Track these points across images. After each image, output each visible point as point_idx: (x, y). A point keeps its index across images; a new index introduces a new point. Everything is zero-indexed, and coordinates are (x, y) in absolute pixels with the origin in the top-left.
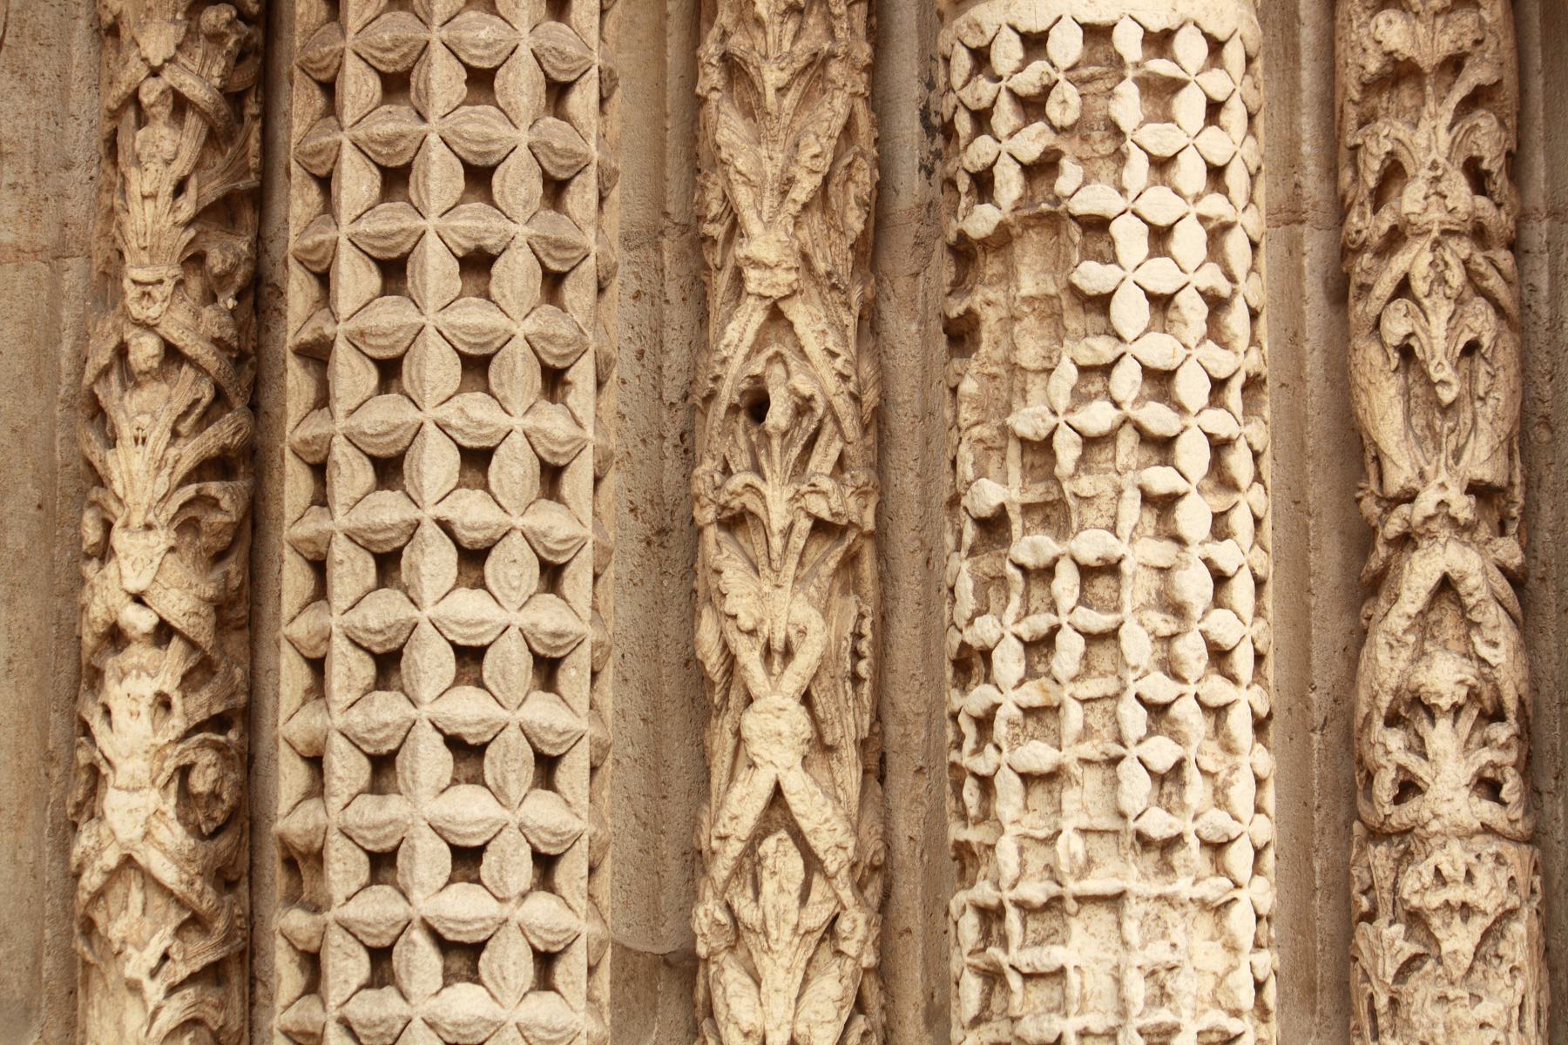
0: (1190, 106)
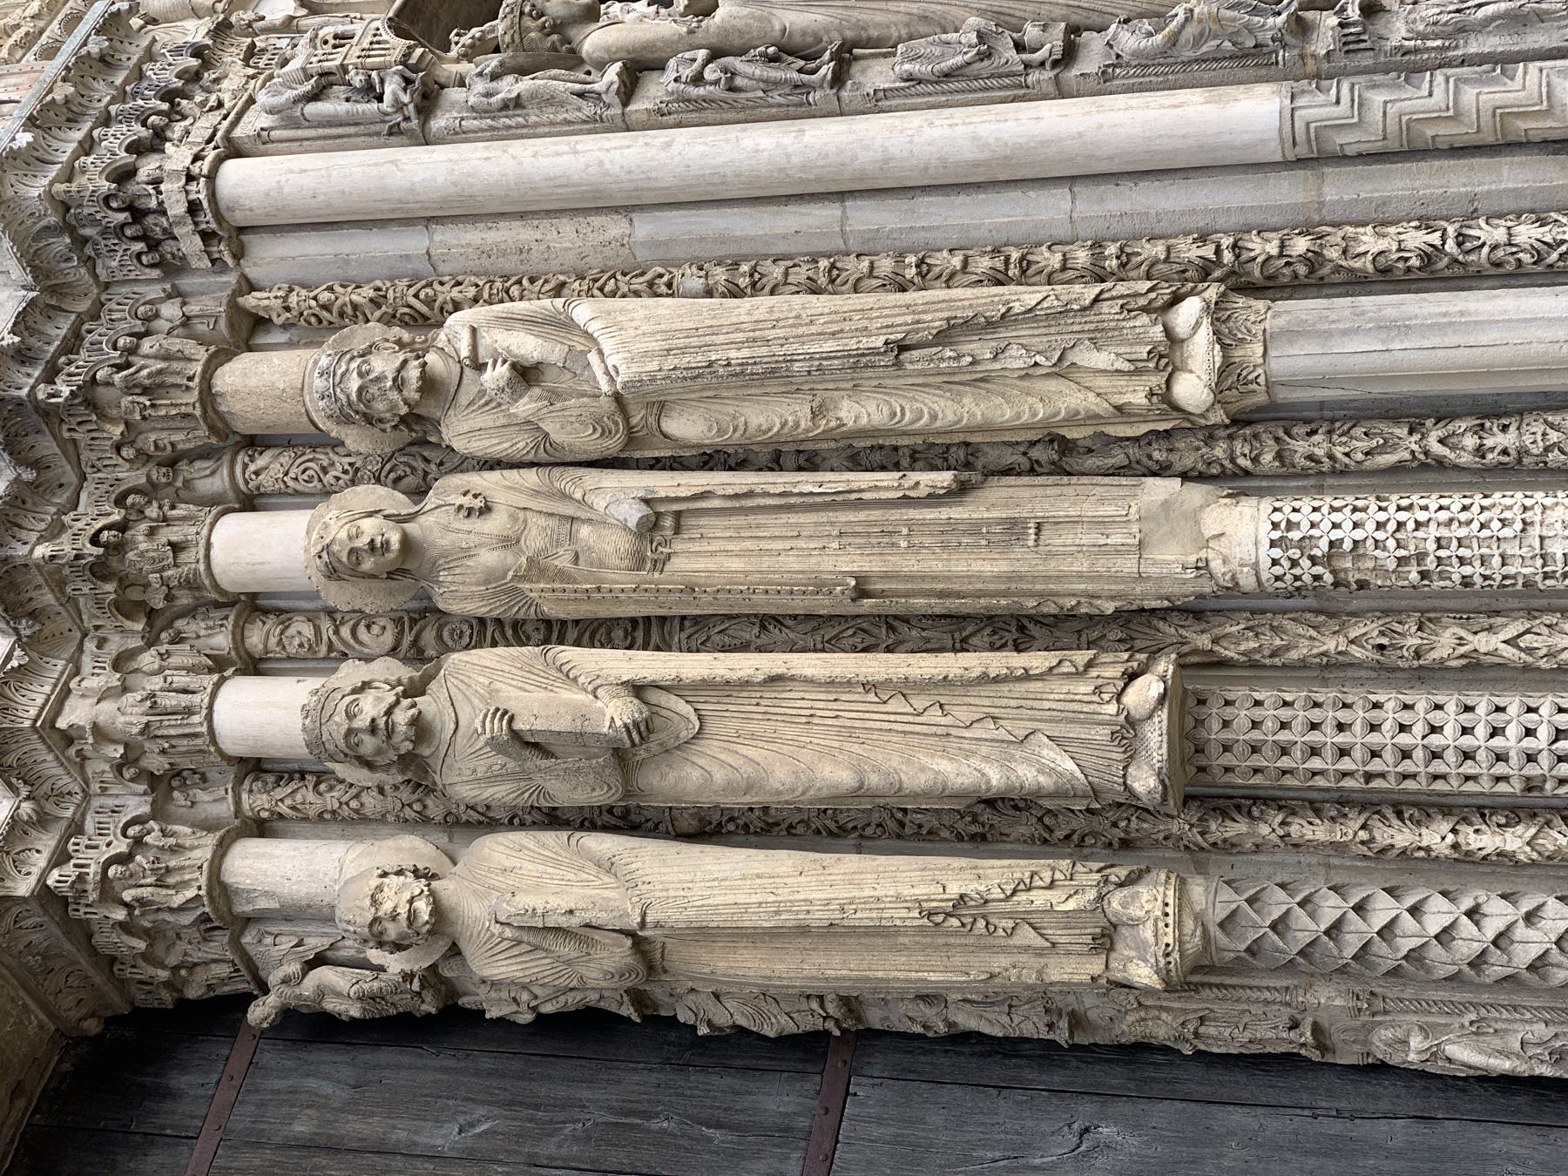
0: (1295, 517)
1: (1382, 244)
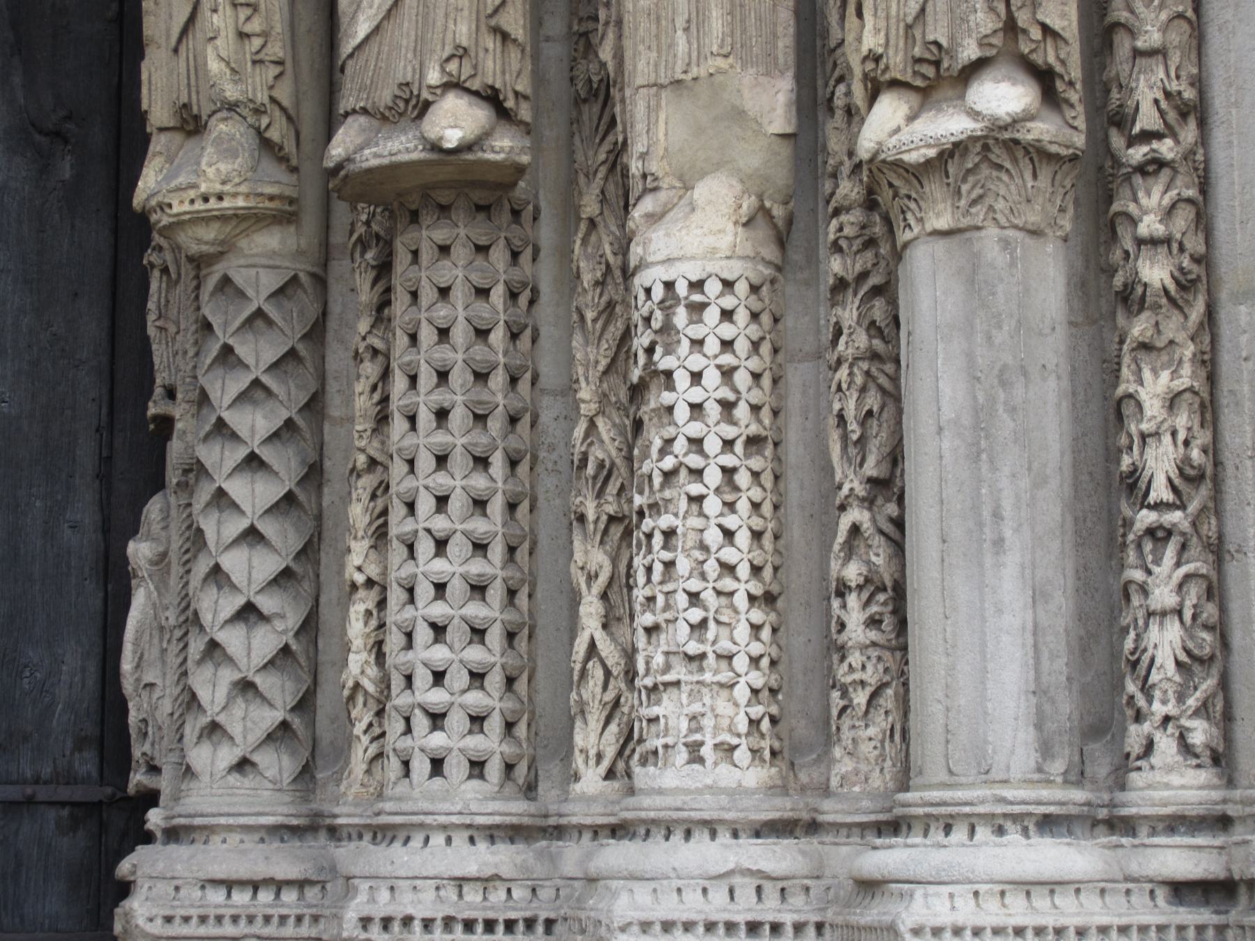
0: (712, 315)
1: (1153, 407)
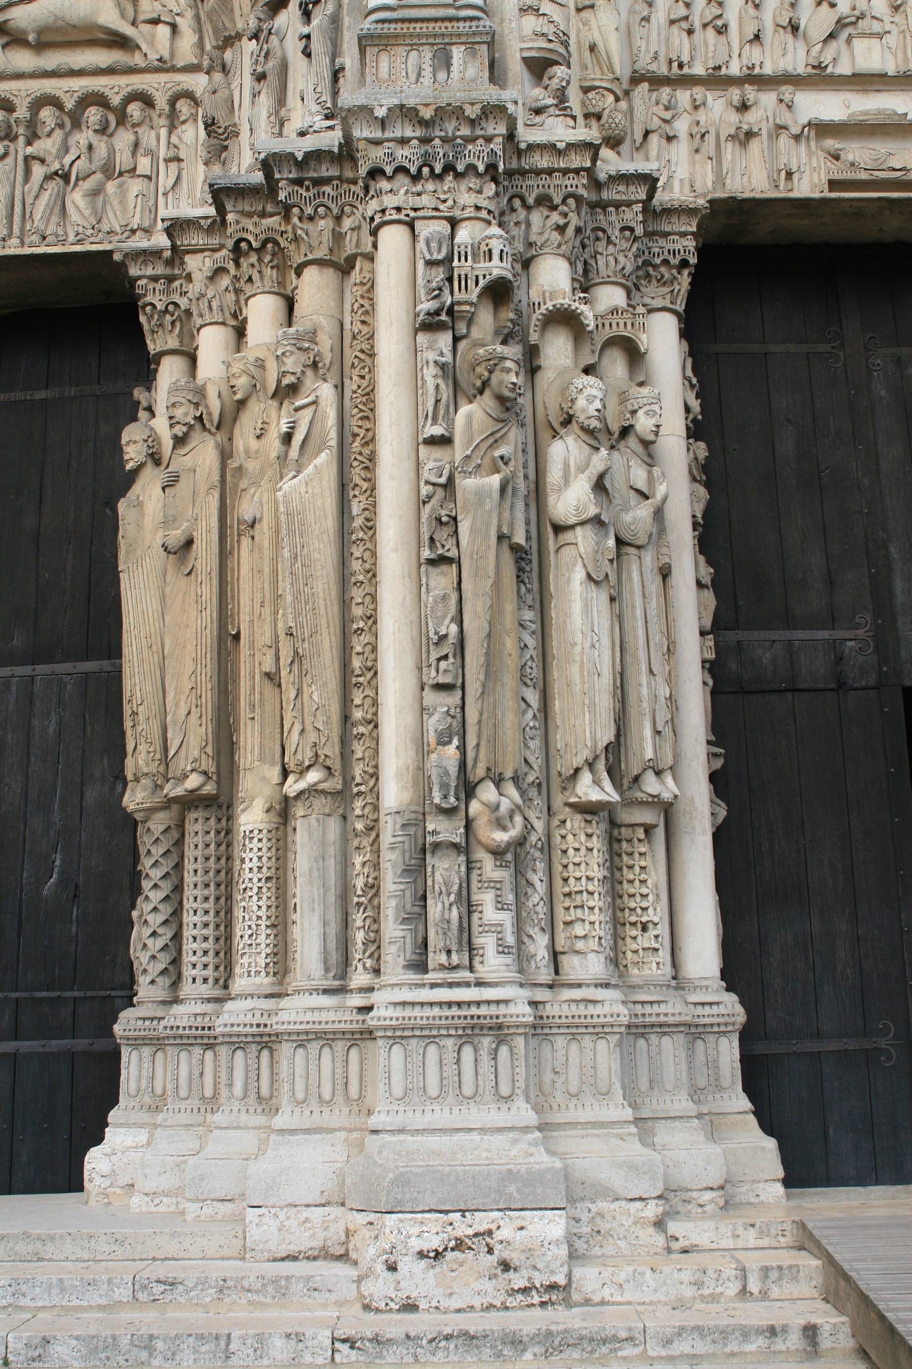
1: (358, 866)
